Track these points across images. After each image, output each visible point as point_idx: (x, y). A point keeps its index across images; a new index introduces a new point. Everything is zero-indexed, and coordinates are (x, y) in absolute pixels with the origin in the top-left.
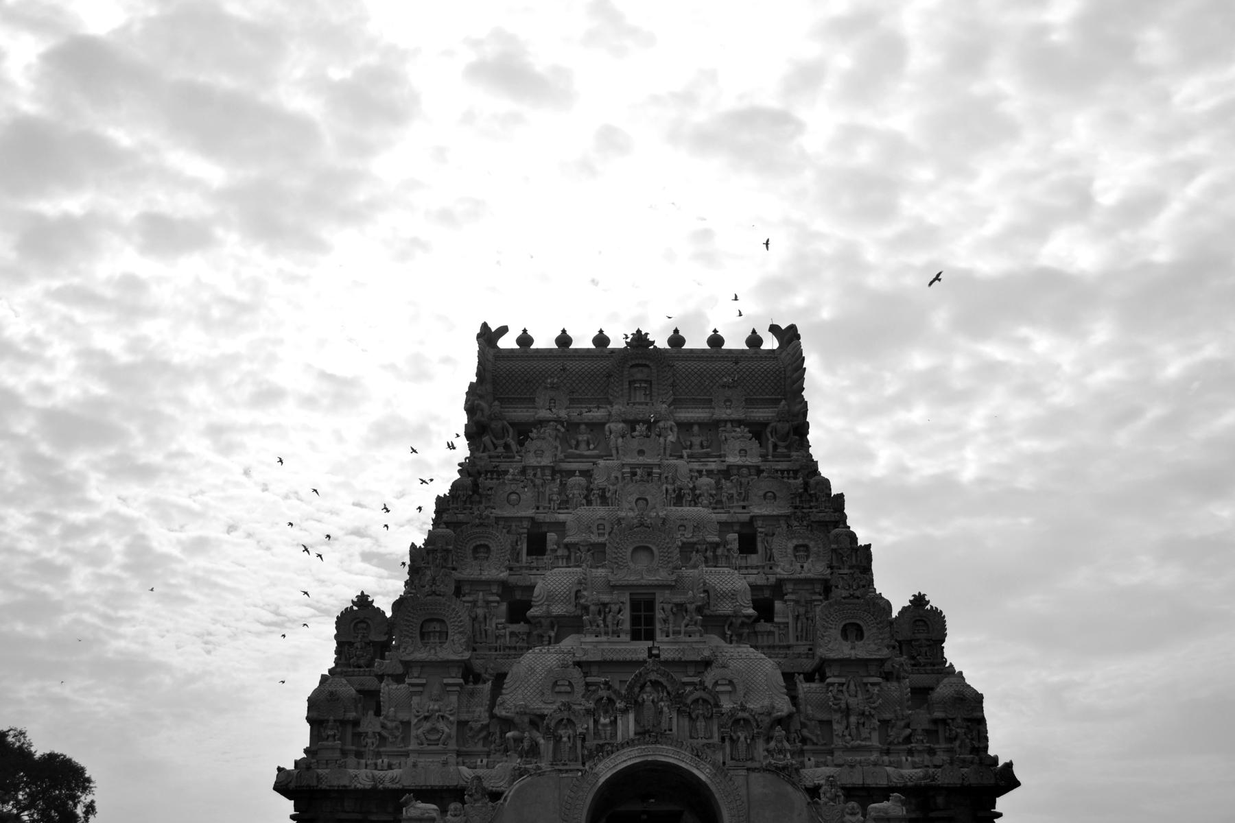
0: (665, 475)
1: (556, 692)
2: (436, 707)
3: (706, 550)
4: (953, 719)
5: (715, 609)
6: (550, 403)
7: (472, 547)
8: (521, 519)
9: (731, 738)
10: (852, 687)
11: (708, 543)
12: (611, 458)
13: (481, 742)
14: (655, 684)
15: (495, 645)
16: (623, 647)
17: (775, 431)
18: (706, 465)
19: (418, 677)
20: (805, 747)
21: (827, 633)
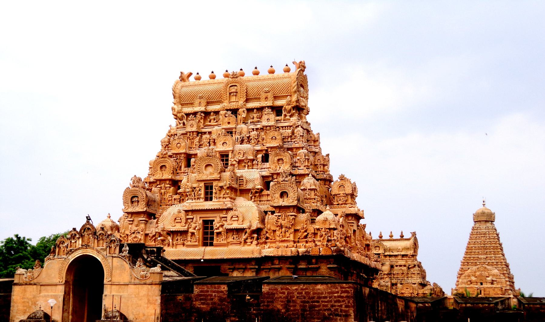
0: (238, 132)
1: (176, 222)
2: (136, 229)
3: (248, 162)
4: (322, 229)
5: (245, 186)
6: (199, 104)
7: (160, 166)
8: (181, 154)
9: (109, 247)
10: (283, 217)
11: (249, 159)
12: (219, 126)
13: (154, 241)
14: (89, 229)
15: (168, 204)
16: (200, 204)
17: (285, 109)
18: (257, 126)
19: (130, 218)
20: (267, 241)
21: (274, 196)
